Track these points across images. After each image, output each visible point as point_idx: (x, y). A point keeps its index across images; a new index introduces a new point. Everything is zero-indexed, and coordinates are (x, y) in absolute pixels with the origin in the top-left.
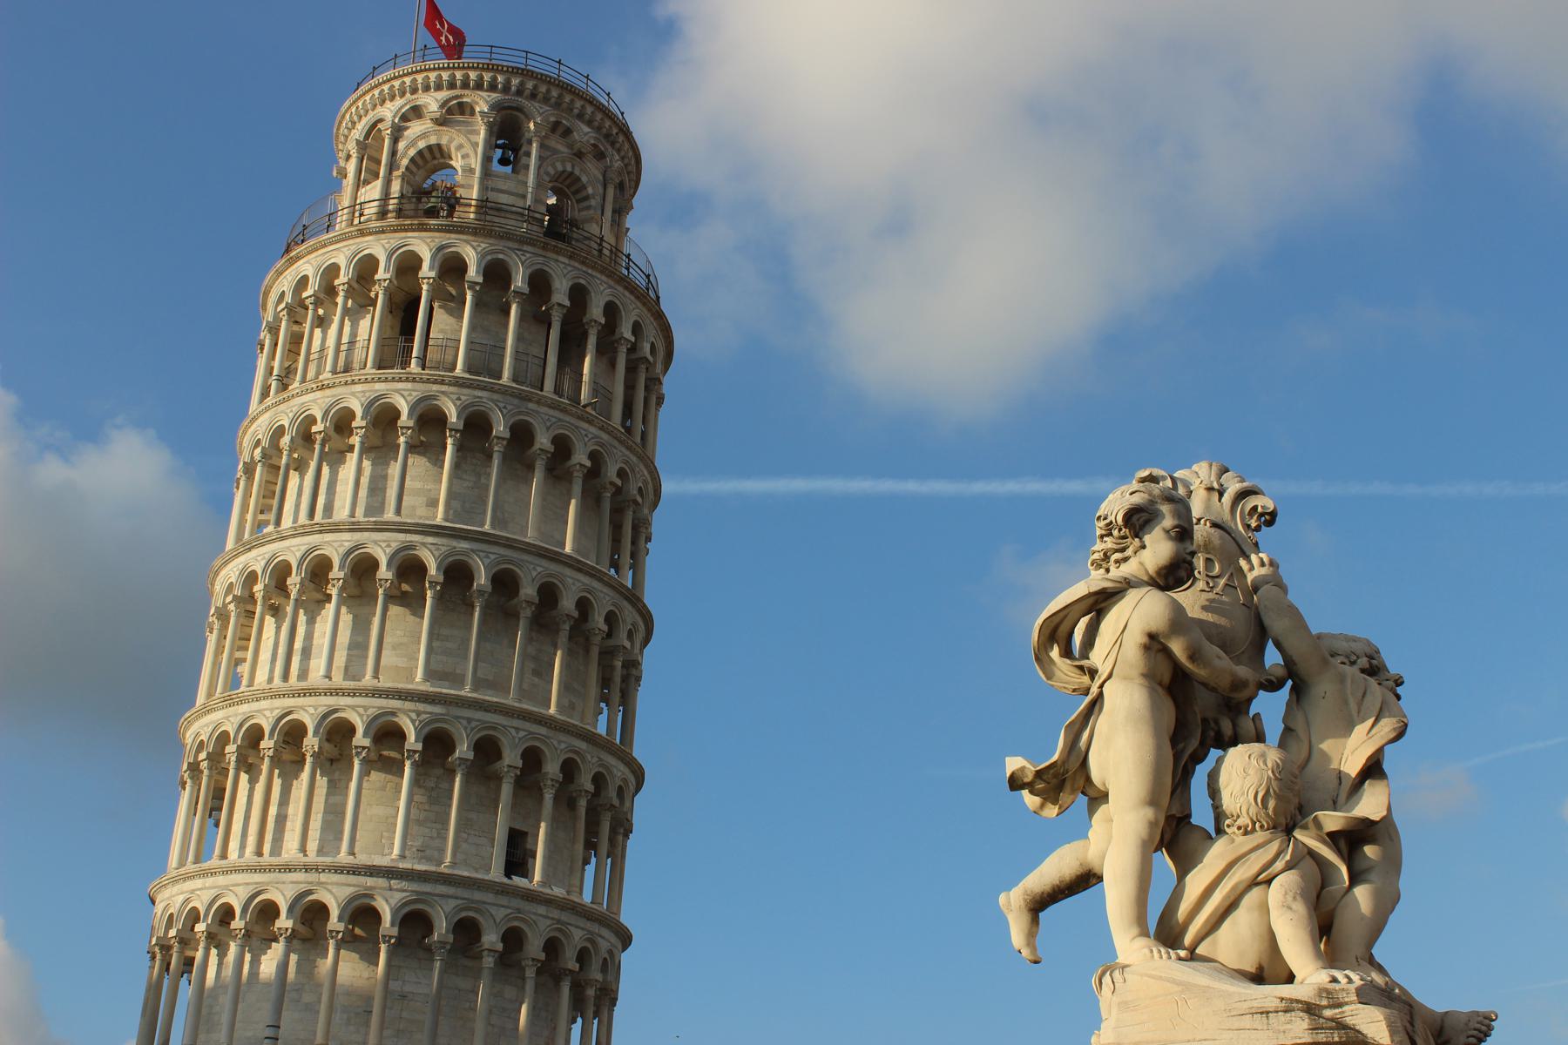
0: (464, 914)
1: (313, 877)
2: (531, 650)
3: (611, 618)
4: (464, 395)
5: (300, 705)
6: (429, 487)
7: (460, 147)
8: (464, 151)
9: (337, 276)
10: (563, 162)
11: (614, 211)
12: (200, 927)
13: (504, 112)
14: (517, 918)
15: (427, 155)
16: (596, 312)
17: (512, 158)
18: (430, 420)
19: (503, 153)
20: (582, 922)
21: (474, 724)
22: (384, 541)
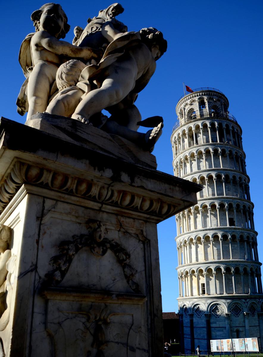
1: (197, 233)
2: (227, 187)
3: (240, 178)
7: (195, 107)
8: (195, 108)
9: (180, 135)
10: (213, 104)
12: (182, 244)
15: (190, 110)
16: (224, 126)
18: (200, 153)
20: (246, 231)
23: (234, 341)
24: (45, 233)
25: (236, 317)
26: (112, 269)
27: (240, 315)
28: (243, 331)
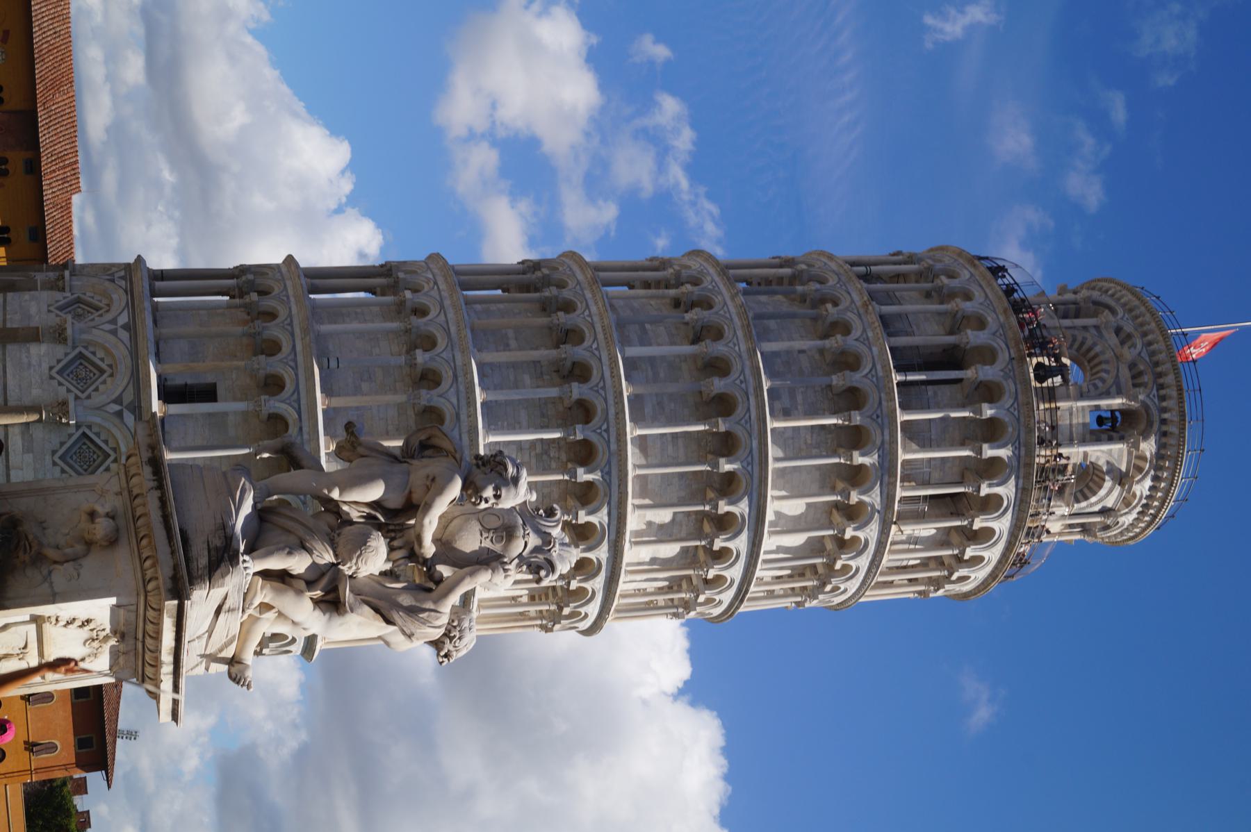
2: (679, 517)
4: (882, 420)
5: (598, 337)
6: (799, 407)
7: (1103, 381)
8: (1100, 384)
11: (1082, 525)
13: (1143, 411)
17: (1104, 427)
19: (1106, 419)
22: (745, 378)
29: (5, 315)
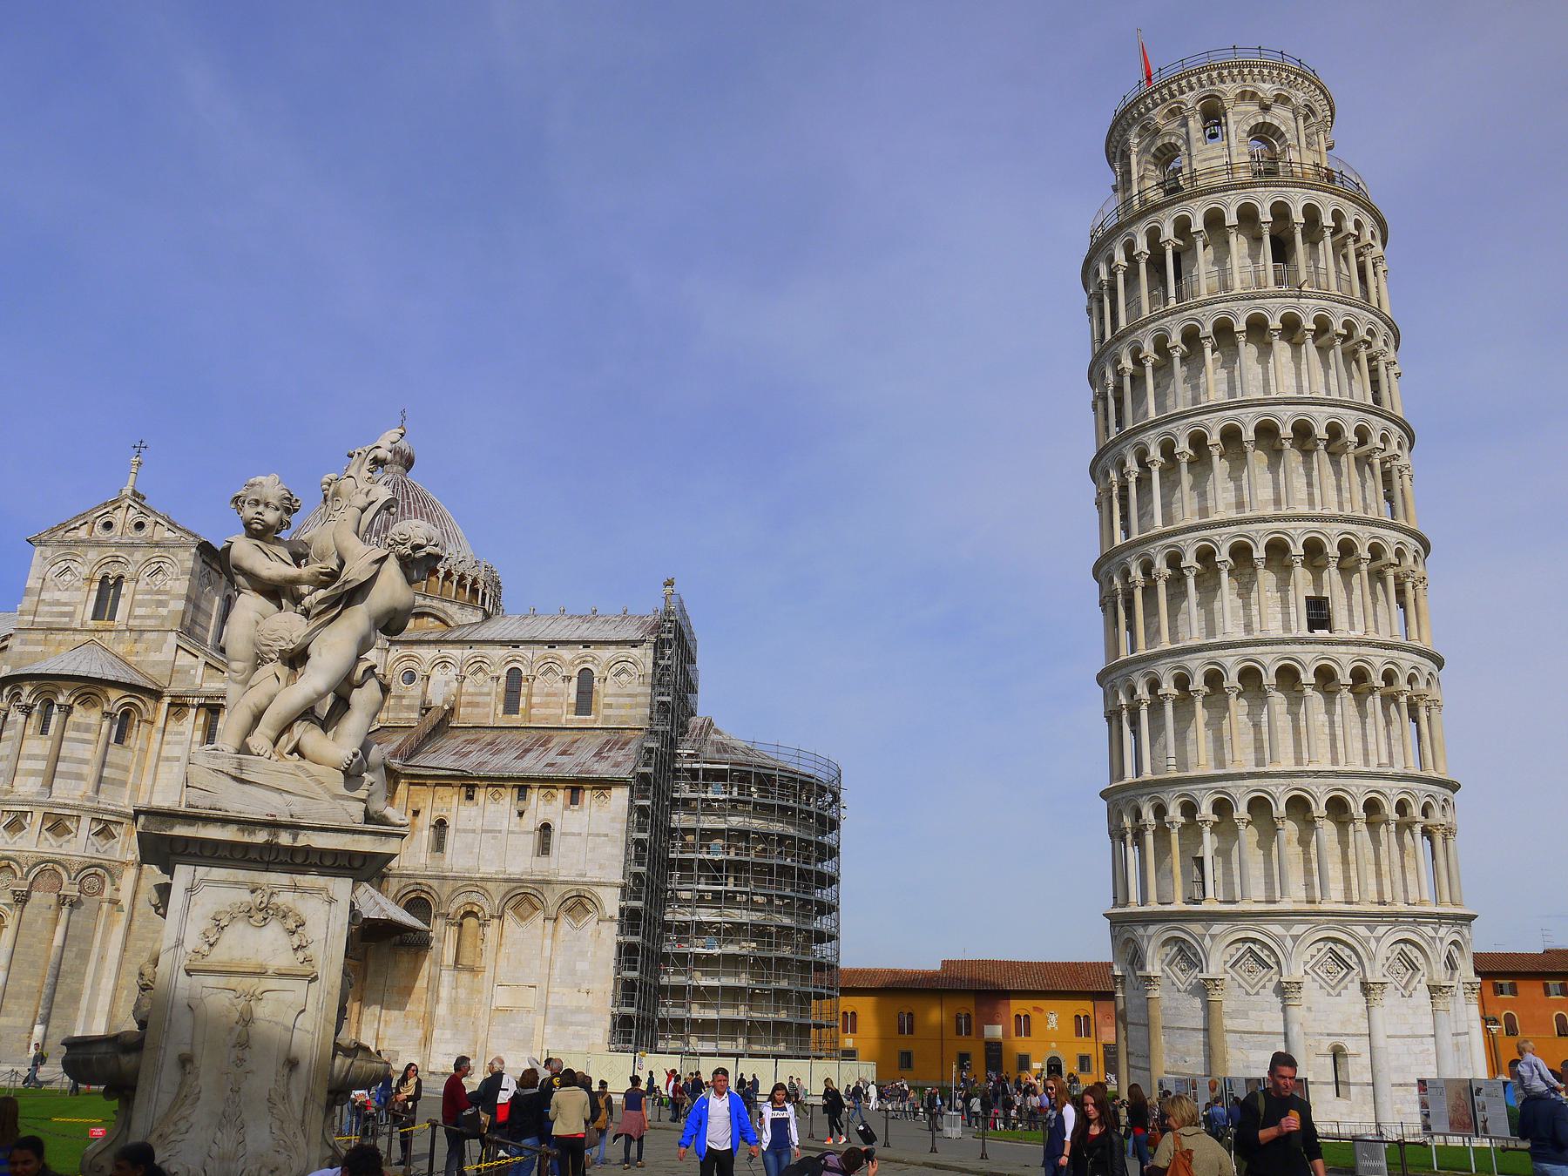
0: (1281, 663)
7: (1177, 141)
14: (1323, 658)
15: (1158, 154)
16: (1298, 217)
18: (1191, 337)
21: (1261, 533)
23: (1231, 1087)
24: (196, 904)
25: (1329, 994)
26: (276, 940)
27: (1346, 988)
28: (1358, 1055)
29: (1141, 1025)
